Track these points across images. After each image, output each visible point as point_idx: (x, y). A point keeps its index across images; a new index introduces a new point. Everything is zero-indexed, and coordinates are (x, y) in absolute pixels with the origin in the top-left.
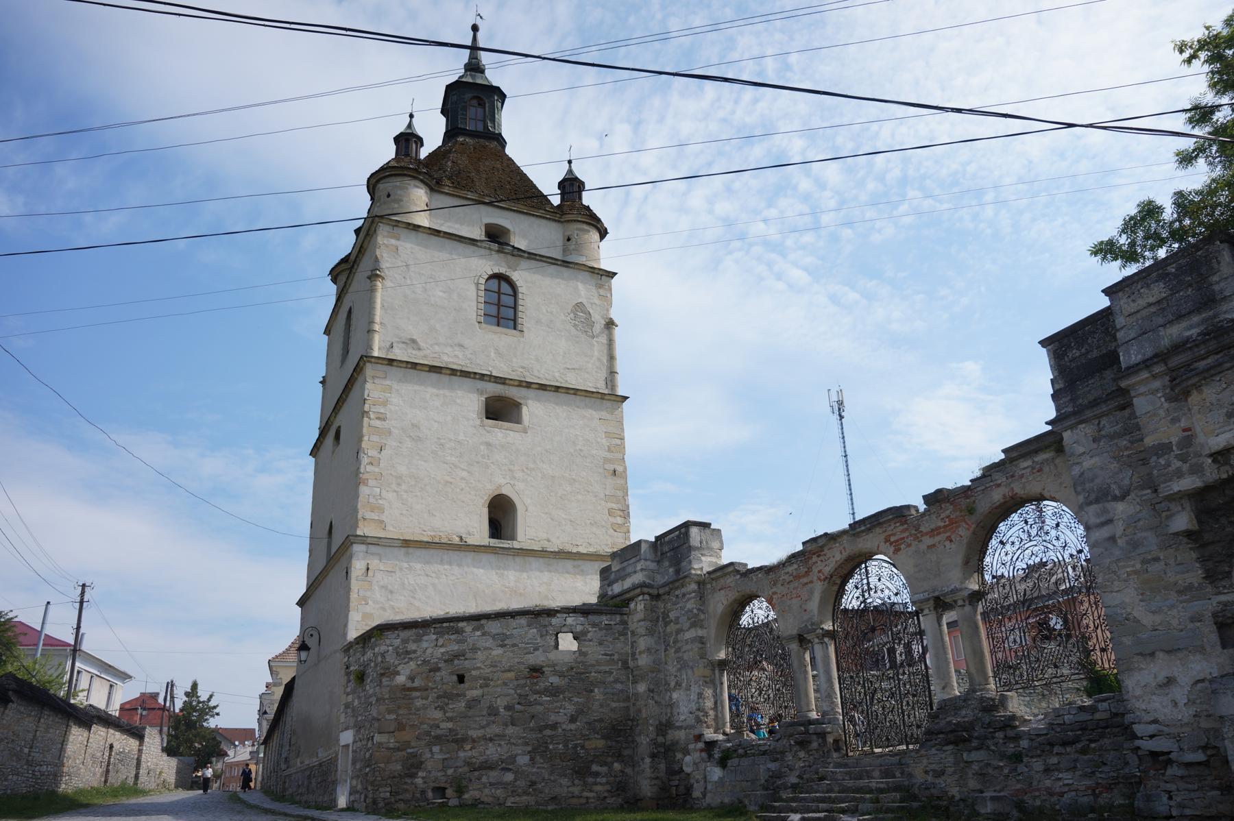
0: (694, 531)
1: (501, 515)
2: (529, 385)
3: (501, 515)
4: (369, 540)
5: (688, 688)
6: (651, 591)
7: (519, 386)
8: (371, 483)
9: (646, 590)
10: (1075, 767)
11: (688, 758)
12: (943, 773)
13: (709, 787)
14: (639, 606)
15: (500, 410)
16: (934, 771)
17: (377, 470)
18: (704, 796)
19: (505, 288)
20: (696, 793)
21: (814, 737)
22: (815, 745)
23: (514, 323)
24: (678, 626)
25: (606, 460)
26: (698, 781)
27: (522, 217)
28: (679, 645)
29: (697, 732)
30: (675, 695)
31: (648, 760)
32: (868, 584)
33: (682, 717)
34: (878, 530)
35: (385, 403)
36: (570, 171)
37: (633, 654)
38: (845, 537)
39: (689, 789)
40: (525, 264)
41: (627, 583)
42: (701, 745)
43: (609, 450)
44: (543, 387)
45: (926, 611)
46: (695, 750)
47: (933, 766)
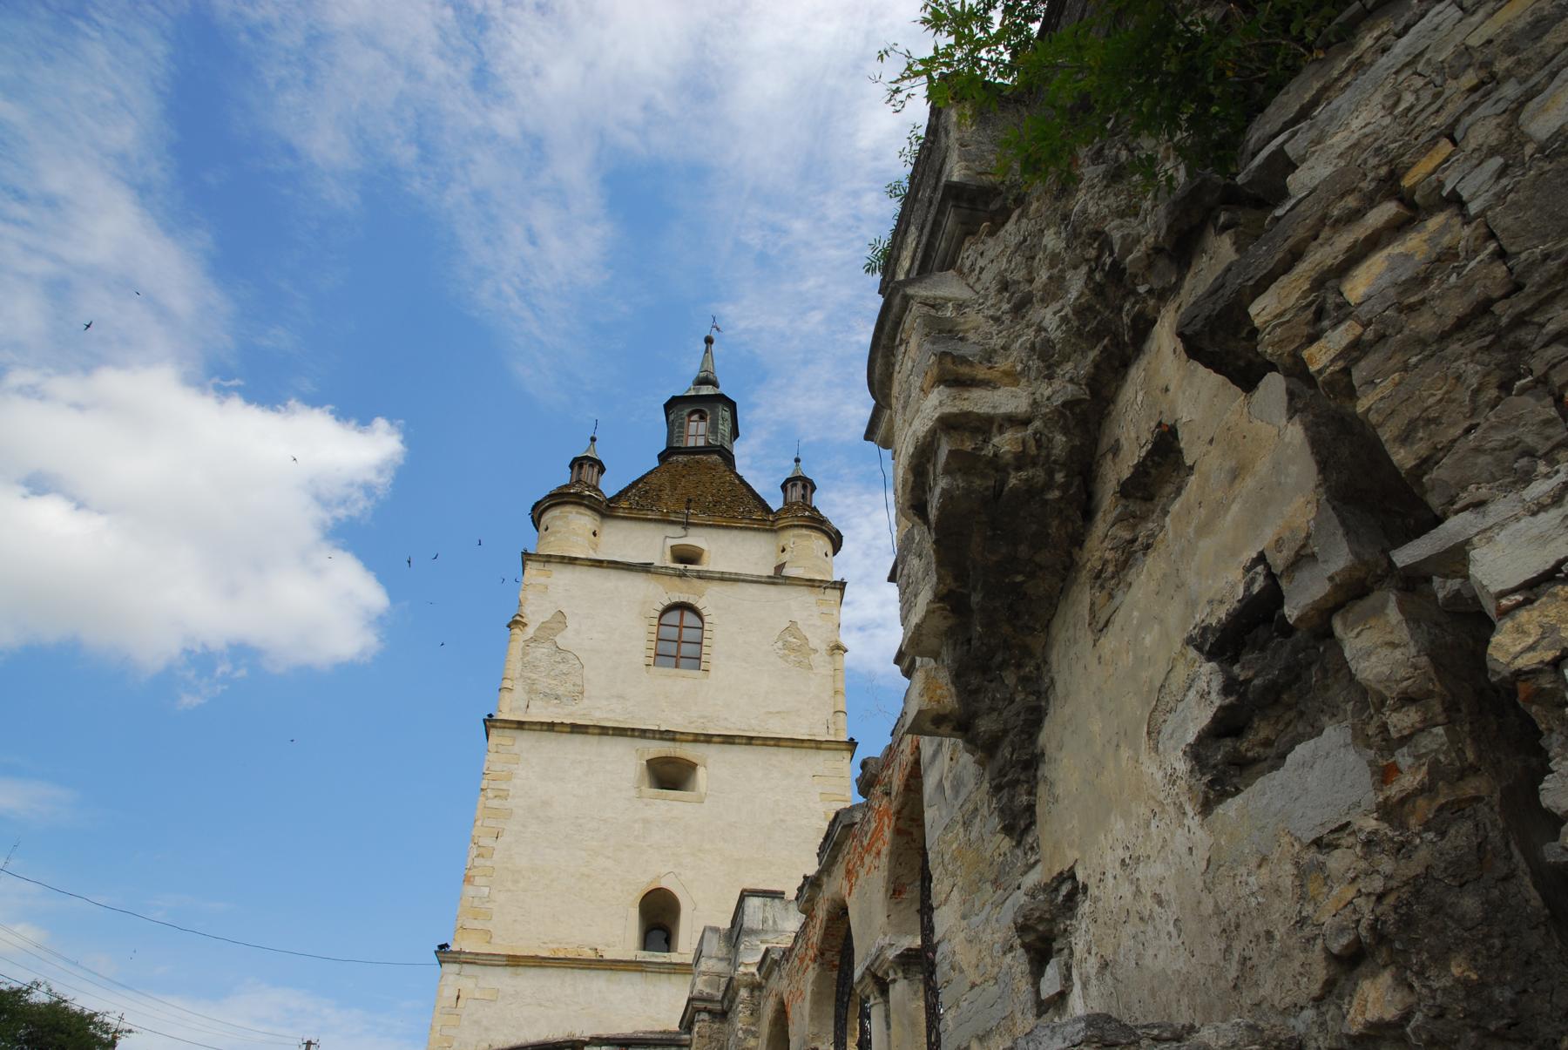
0: (753, 903)
1: (659, 916)
2: (708, 739)
3: (659, 916)
4: (462, 957)
6: (710, 1006)
7: (695, 741)
8: (478, 881)
15: (670, 775)
17: (488, 863)
19: (689, 619)
23: (696, 661)
27: (721, 532)
35: (510, 777)
36: (796, 470)
40: (715, 589)
44: (729, 740)
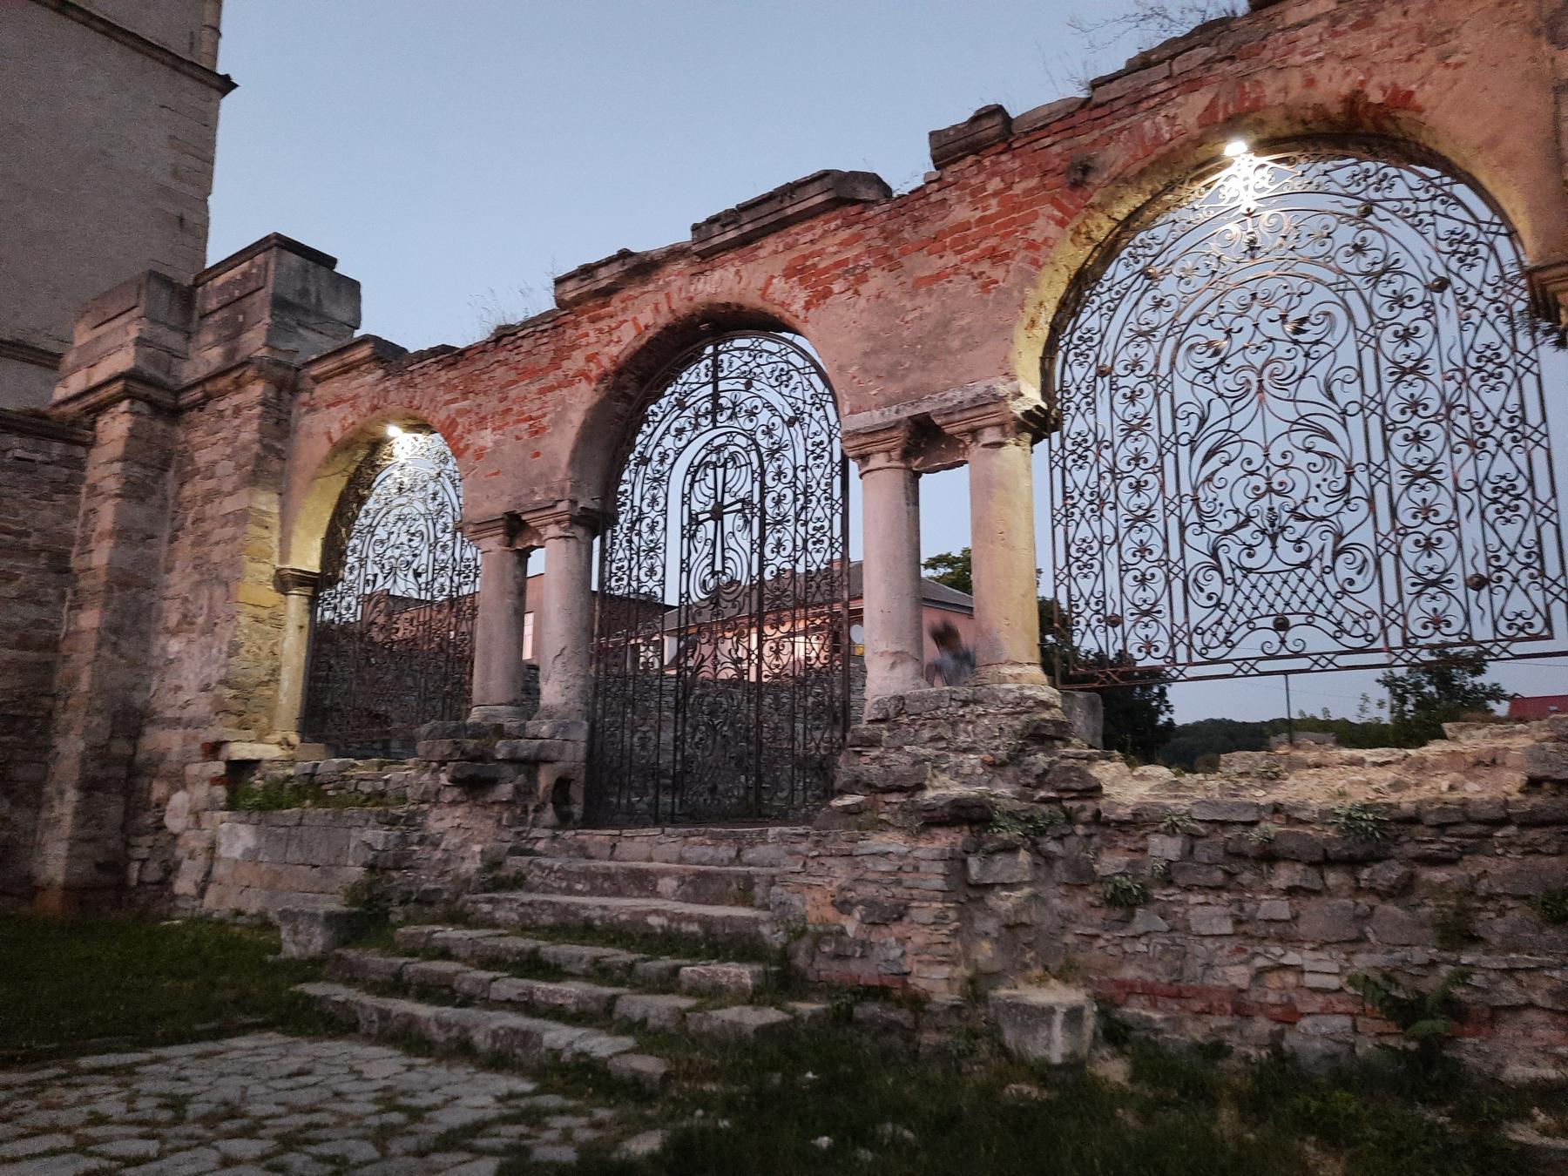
5: (210, 628)
6: (155, 394)
9: (138, 388)
10: (1362, 939)
11: (179, 799)
12: (899, 913)
13: (220, 870)
14: (116, 427)
16: (870, 904)
18: (202, 892)
20: (184, 885)
21: (508, 770)
22: (505, 791)
24: (211, 484)
25: (164, 191)
26: (192, 856)
28: (206, 526)
29: (211, 735)
30: (175, 646)
31: (72, 795)
32: (715, 395)
33: (184, 697)
34: (771, 244)
37: (86, 540)
38: (682, 265)
39: (171, 870)
41: (100, 374)
42: (218, 768)
43: (175, 174)
45: (878, 461)
46: (199, 779)
47: (869, 891)
